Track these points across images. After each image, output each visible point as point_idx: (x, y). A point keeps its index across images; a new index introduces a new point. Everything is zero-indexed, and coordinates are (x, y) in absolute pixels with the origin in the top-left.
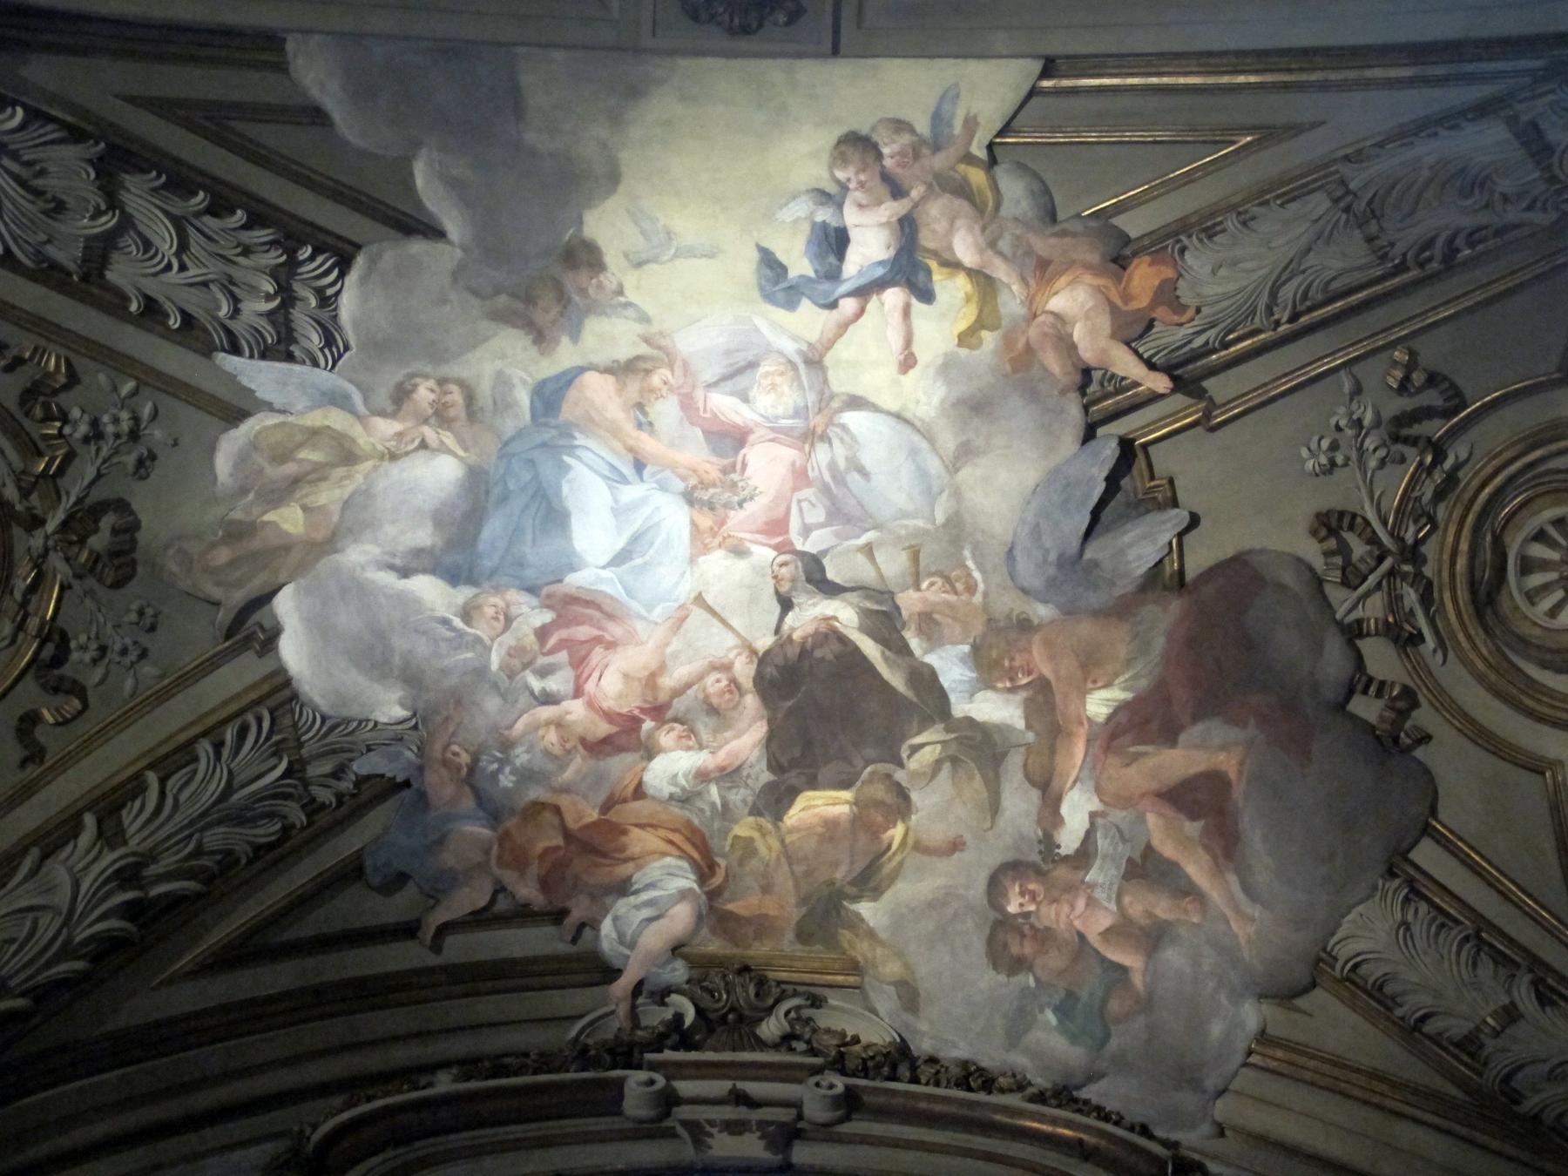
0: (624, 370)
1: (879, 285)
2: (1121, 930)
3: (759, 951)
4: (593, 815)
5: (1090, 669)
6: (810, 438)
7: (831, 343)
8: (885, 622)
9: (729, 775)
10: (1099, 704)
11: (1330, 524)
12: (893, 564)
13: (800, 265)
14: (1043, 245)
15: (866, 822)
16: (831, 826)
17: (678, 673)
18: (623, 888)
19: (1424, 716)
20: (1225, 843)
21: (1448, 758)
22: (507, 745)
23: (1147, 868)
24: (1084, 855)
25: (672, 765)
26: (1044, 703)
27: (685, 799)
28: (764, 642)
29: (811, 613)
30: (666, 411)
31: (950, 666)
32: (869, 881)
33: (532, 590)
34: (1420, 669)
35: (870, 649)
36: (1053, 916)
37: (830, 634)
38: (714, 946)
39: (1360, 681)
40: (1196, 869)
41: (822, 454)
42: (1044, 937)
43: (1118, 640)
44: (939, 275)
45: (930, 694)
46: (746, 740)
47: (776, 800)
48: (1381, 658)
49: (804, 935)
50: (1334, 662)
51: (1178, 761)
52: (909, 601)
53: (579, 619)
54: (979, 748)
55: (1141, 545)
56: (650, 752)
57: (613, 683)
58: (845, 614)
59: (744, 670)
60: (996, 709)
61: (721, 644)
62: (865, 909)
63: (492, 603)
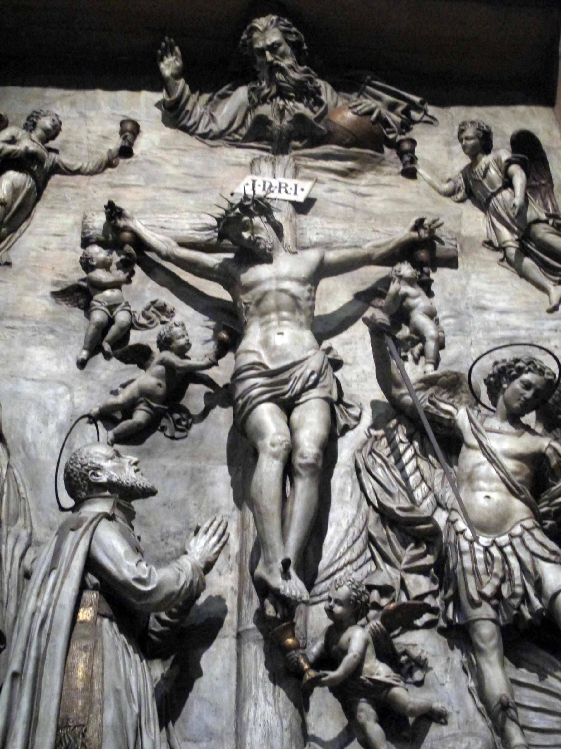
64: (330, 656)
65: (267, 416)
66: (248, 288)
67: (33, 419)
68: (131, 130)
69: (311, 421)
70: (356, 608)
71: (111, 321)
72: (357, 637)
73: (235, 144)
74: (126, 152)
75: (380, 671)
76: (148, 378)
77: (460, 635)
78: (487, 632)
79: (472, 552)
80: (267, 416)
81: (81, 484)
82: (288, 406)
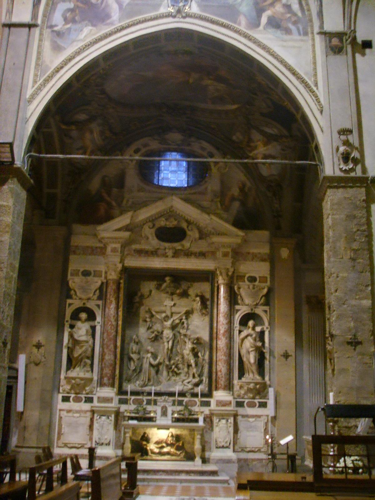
64: (171, 368)
65: (166, 344)
66: (165, 325)
67: (142, 338)
68: (151, 291)
69: (170, 343)
70: (174, 364)
71: (149, 326)
72: (173, 367)
73: (164, 293)
74: (150, 294)
75: (176, 369)
76: (153, 335)
77: (184, 364)
78: (186, 365)
79: (186, 357)
80: (166, 344)
81: (148, 352)
82: (168, 342)
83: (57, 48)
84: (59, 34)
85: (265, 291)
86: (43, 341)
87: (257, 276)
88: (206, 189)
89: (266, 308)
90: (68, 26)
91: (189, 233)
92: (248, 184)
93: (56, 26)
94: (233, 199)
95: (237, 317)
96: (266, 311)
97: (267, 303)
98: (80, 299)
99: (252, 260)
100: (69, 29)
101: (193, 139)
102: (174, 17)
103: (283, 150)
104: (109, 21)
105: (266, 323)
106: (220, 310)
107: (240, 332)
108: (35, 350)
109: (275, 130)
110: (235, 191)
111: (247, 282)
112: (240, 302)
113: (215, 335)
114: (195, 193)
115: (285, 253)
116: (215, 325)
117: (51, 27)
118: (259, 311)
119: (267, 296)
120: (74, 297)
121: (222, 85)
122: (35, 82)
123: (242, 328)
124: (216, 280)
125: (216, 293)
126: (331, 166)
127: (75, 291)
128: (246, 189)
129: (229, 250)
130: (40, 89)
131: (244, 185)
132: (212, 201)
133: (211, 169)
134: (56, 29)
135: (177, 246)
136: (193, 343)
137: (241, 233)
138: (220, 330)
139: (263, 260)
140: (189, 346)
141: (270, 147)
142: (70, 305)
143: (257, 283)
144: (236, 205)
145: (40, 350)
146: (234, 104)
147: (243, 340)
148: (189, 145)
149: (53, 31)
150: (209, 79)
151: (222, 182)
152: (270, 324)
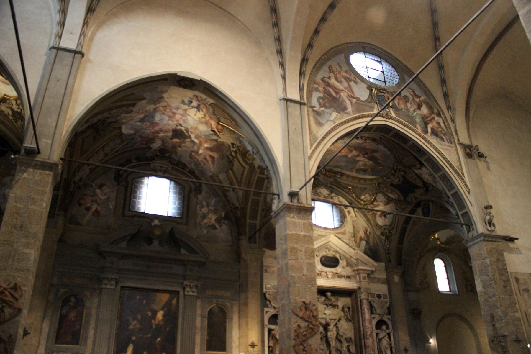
0: (163, 107)
1: (194, 108)
2: (202, 161)
3: (167, 148)
4: (152, 137)
5: (206, 142)
6: (183, 116)
7: (187, 109)
8: (187, 130)
9: (168, 136)
10: (206, 145)
11: (232, 144)
12: (189, 127)
13: (186, 102)
14: (212, 116)
15: (180, 142)
16: (177, 142)
17: (164, 128)
18: (154, 143)
19: (235, 159)
20: (213, 162)
21: (236, 163)
22: (144, 133)
23: (205, 159)
24: (201, 154)
25: (161, 135)
26: (200, 142)
27: (162, 137)
28: (174, 128)
29: (179, 127)
30: (168, 110)
31: (193, 136)
32: (180, 146)
33: (150, 122)
34: (236, 156)
35: (185, 131)
36: (196, 157)
37: (181, 129)
38: (162, 147)
39: (231, 155)
40: (210, 162)
41: (184, 118)
42: (195, 158)
43: (210, 142)
44: (201, 111)
45: (190, 137)
46: (170, 134)
47: (172, 139)
48: (233, 154)
49: (172, 148)
50: (229, 153)
51: (212, 154)
52: (190, 130)
53: (154, 124)
54: (193, 142)
55: (215, 137)
56: (159, 133)
57: (156, 129)
58: (183, 129)
59: (171, 129)
60: (196, 141)
61: (169, 127)
62: (179, 148)
63: (145, 123)
79: (343, 352)
83: (320, 124)
84: (317, 113)
85: (388, 304)
86: (256, 342)
87: (381, 294)
88: (345, 230)
89: (389, 317)
90: (322, 109)
91: (340, 261)
92: (369, 230)
93: (315, 107)
94: (361, 239)
95: (374, 323)
96: (389, 319)
97: (389, 313)
98: (274, 308)
99: (378, 282)
100: (323, 111)
101: (333, 194)
102: (384, 117)
103: (396, 209)
104: (346, 111)
105: (391, 327)
106: (365, 318)
107: (377, 334)
108: (250, 349)
109: (396, 196)
110: (362, 234)
111: (376, 298)
112: (374, 312)
113: (362, 336)
114: (339, 233)
115: (396, 279)
116: (362, 328)
117: (312, 107)
118: (386, 318)
119: (389, 308)
120: (270, 306)
121: (371, 162)
122: (311, 145)
123: (378, 331)
124: (358, 296)
125: (359, 306)
126: (481, 228)
127: (270, 301)
128: (368, 233)
129: (366, 275)
130: (314, 151)
131: (366, 230)
132: (350, 239)
133: (346, 217)
134: (315, 109)
135: (333, 270)
136: (347, 342)
137: (375, 264)
138: (367, 333)
139: (383, 283)
140: (345, 344)
141: (388, 206)
142: (267, 312)
143: (382, 299)
144: (364, 243)
145: (254, 349)
146: (373, 175)
147: (380, 340)
148: (332, 198)
149: (314, 110)
150: (365, 157)
151: (354, 227)
152: (393, 328)
